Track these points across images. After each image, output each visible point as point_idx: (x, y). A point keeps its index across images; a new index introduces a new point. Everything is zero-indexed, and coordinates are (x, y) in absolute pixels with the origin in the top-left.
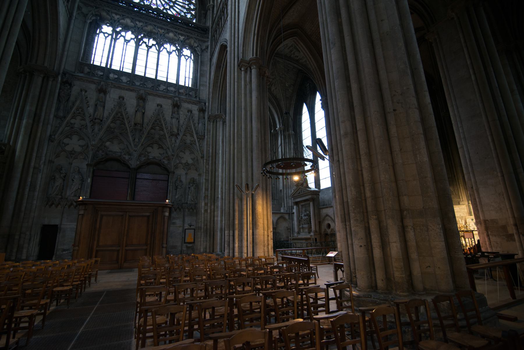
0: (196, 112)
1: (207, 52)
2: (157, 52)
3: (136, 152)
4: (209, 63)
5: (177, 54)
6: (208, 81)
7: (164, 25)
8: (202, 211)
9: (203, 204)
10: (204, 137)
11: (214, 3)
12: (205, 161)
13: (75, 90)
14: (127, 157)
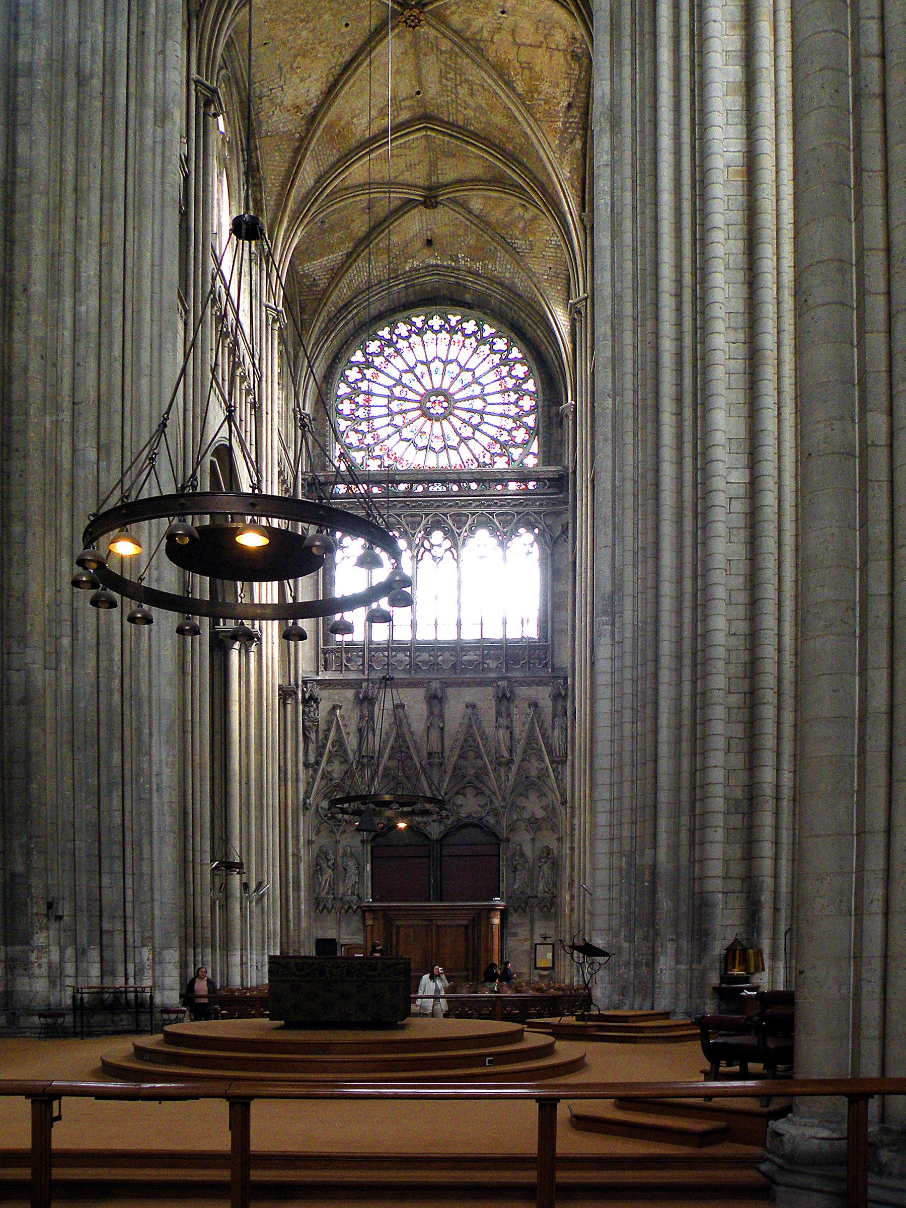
1: (566, 541)
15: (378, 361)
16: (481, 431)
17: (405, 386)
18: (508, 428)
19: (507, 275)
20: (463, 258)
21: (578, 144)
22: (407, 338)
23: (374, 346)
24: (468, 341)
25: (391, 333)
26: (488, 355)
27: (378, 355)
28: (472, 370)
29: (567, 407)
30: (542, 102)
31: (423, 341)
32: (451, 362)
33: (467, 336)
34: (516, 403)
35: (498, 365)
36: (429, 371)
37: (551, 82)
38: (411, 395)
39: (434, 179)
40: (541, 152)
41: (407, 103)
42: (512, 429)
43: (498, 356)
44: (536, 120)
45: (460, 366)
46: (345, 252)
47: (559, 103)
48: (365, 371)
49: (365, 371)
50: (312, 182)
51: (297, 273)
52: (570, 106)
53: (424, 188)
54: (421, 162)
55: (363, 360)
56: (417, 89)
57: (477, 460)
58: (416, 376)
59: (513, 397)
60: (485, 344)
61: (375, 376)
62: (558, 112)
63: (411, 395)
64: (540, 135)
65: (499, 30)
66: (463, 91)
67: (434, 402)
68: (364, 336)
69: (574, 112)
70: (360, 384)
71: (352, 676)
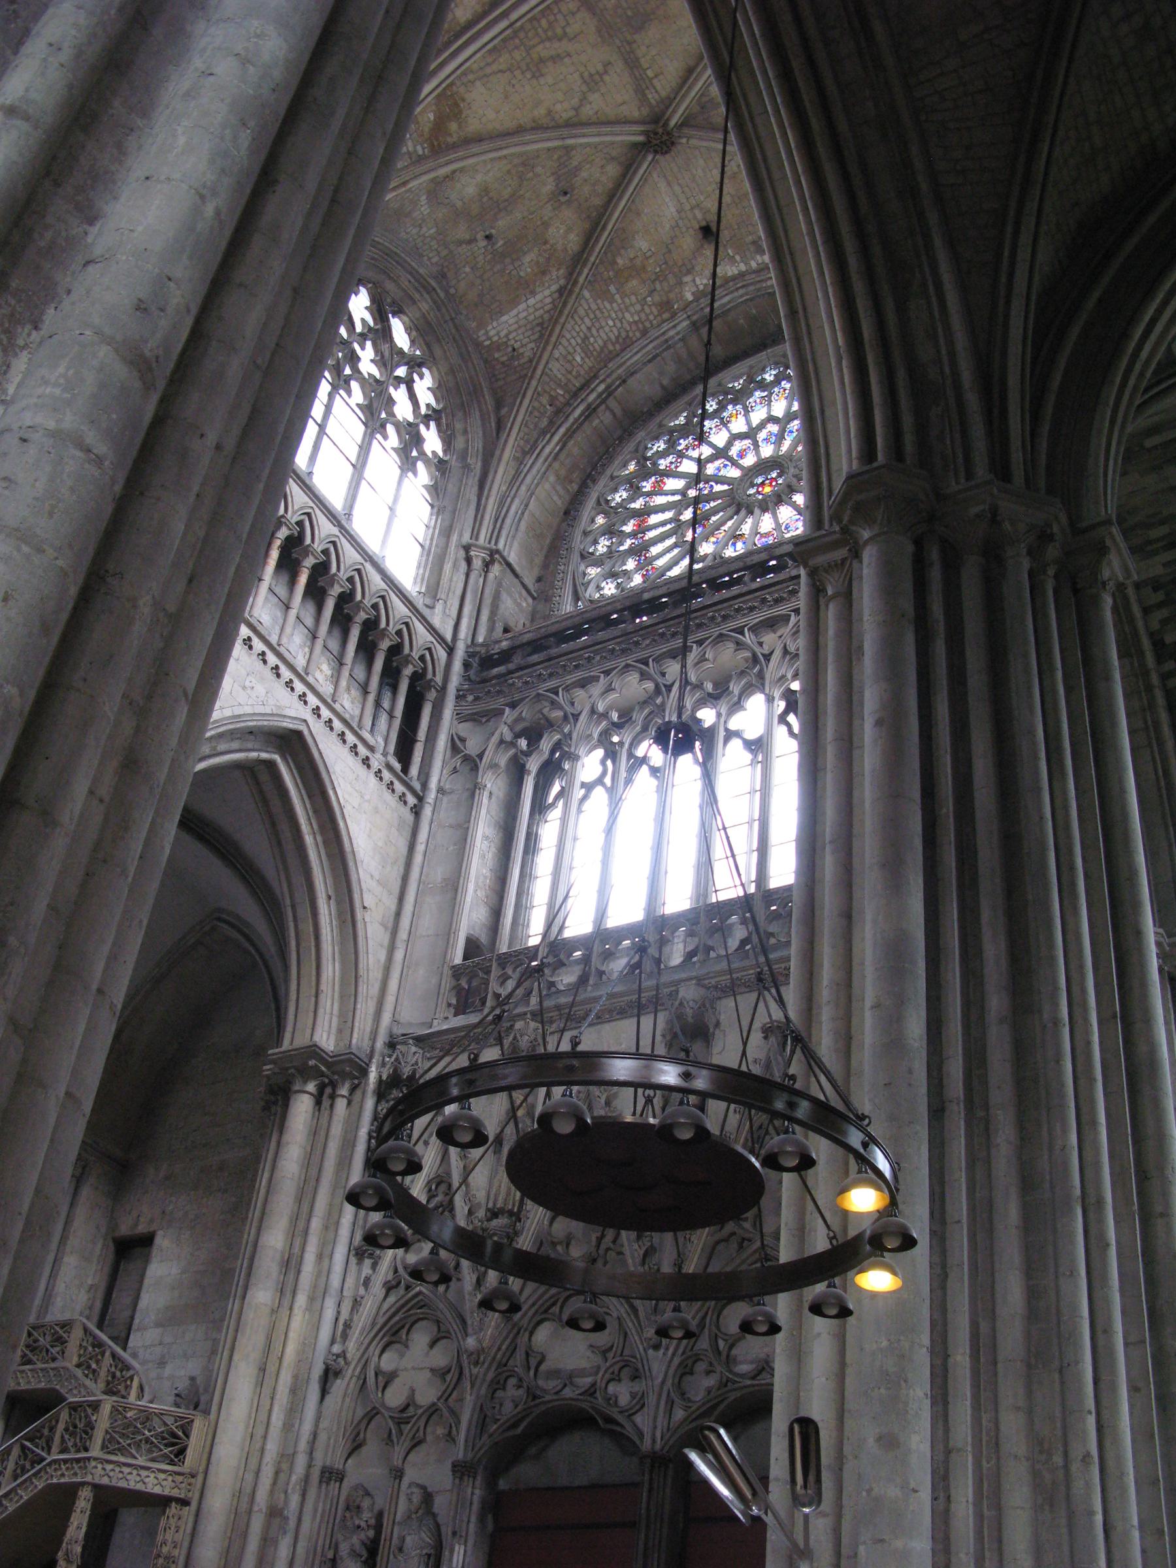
3: (662, 1351)
7: (777, 601)
14: (622, 1392)
39: (652, 97)
46: (554, 287)
51: (478, 345)
53: (643, 123)
54: (607, 65)
67: (763, 484)
68: (641, 434)
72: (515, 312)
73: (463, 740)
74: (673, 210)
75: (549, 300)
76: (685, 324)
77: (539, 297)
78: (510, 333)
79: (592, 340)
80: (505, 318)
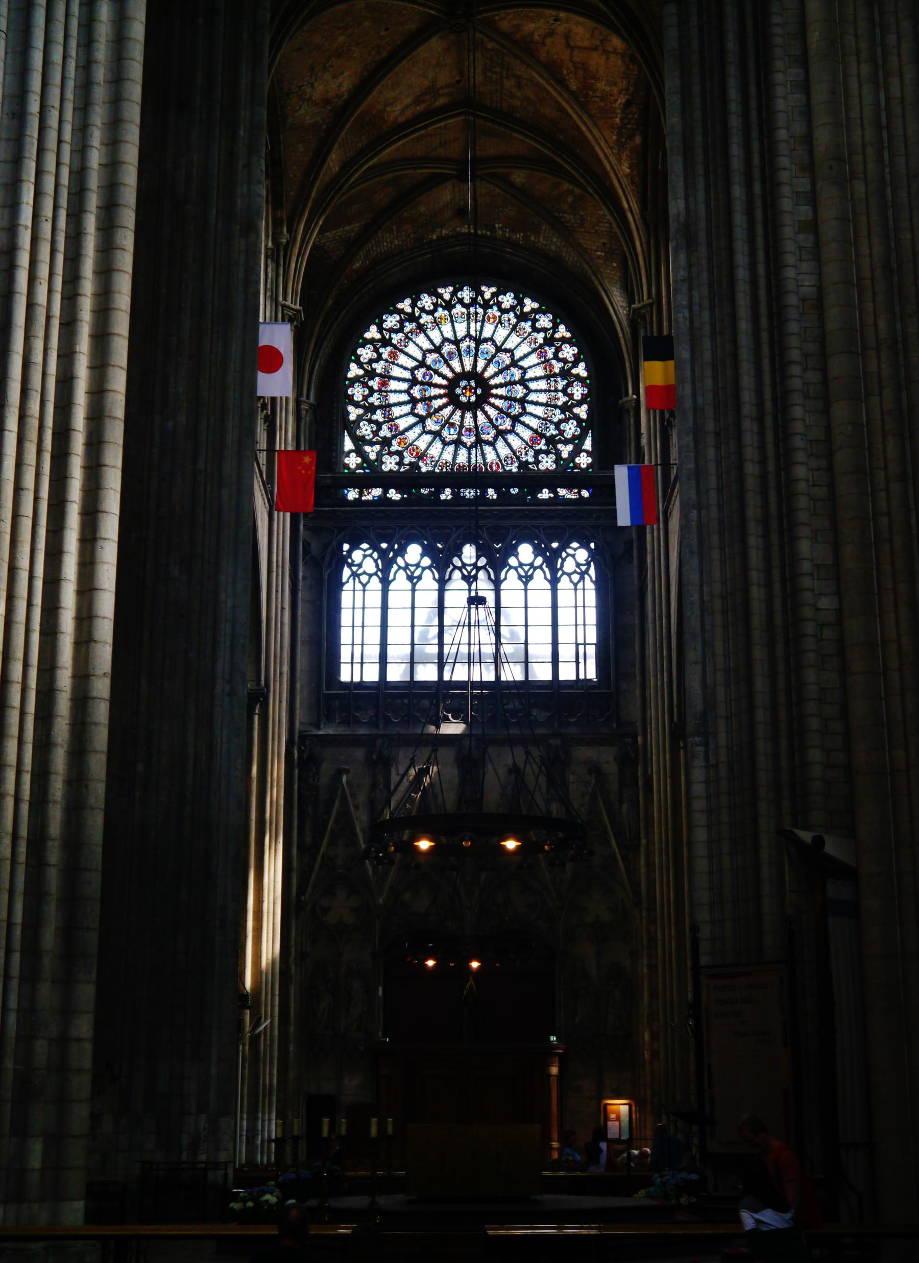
0: (611, 768)
2: (492, 587)
4: (637, 603)
5: (549, 577)
6: (638, 666)
8: (646, 1056)
9: (647, 1037)
10: (640, 840)
11: (638, 394)
12: (644, 914)
13: (326, 770)
15: (396, 338)
16: (523, 424)
17: (429, 368)
18: (555, 420)
19: (553, 248)
20: (500, 228)
21: (638, 140)
22: (431, 313)
23: (391, 321)
24: (505, 316)
25: (413, 305)
26: (529, 334)
27: (397, 332)
28: (511, 351)
29: (627, 402)
30: (598, 100)
31: (451, 316)
32: (486, 340)
33: (504, 311)
34: (564, 391)
35: (541, 346)
36: (459, 350)
37: (607, 81)
38: (437, 380)
40: (597, 148)
41: (446, 91)
42: (561, 421)
43: (542, 335)
44: (591, 117)
45: (496, 345)
46: (363, 223)
47: (616, 101)
48: (382, 350)
49: (382, 350)
50: (337, 169)
52: (628, 104)
55: (378, 336)
56: (458, 78)
57: (518, 458)
58: (442, 356)
59: (561, 384)
60: (526, 321)
61: (393, 355)
62: (615, 108)
63: (437, 380)
64: (595, 132)
65: (551, 33)
66: (509, 84)
67: (465, 388)
69: (634, 109)
70: (375, 365)
71: (362, 731)
72: (334, 232)
73: (309, 544)
74: (449, 198)
75: (357, 229)
76: (429, 256)
77: (352, 226)
78: (327, 242)
79: (371, 252)
80: (327, 234)
